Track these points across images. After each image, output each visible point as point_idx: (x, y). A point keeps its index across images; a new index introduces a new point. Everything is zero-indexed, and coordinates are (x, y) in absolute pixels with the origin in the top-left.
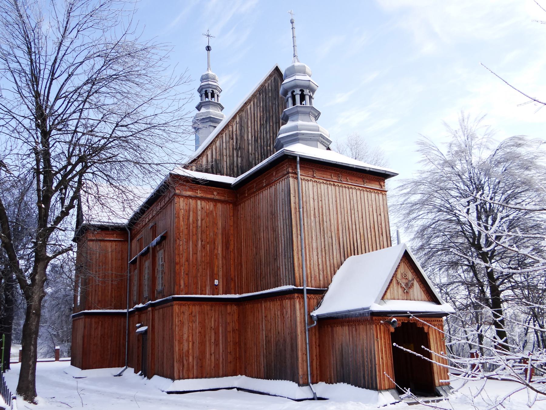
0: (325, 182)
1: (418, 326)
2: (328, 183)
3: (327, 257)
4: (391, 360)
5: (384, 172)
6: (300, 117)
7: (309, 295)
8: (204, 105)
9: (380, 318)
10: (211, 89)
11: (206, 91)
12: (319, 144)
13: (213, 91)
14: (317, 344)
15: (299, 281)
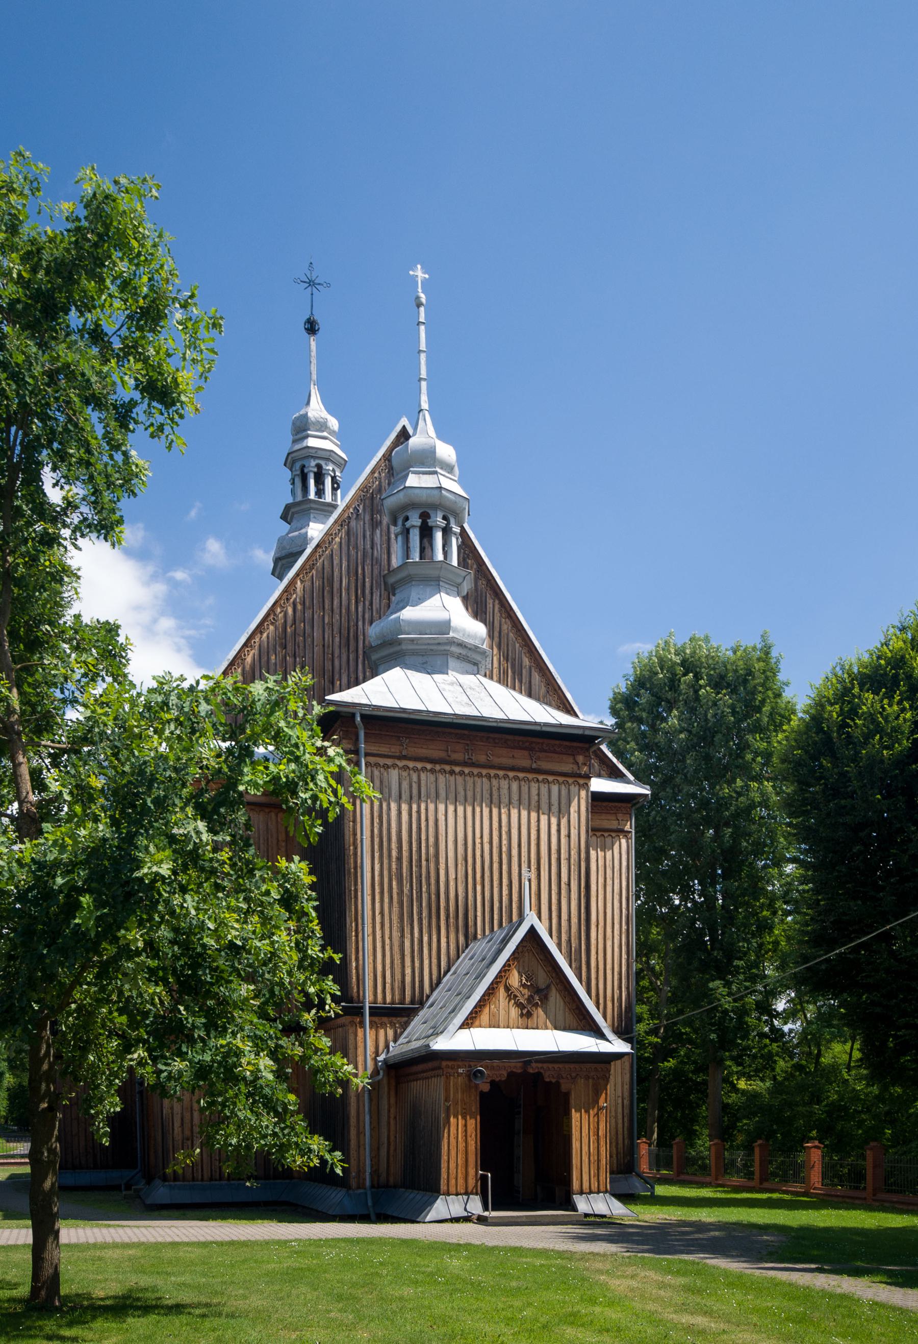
0: (429, 766)
1: (547, 1080)
2: (438, 767)
3: (425, 939)
4: (476, 1143)
5: (580, 732)
6: (414, 593)
7: (376, 1019)
8: (297, 512)
9: (460, 1063)
10: (313, 463)
11: (303, 467)
12: (452, 662)
13: (319, 467)
14: (392, 1116)
15: (355, 990)
